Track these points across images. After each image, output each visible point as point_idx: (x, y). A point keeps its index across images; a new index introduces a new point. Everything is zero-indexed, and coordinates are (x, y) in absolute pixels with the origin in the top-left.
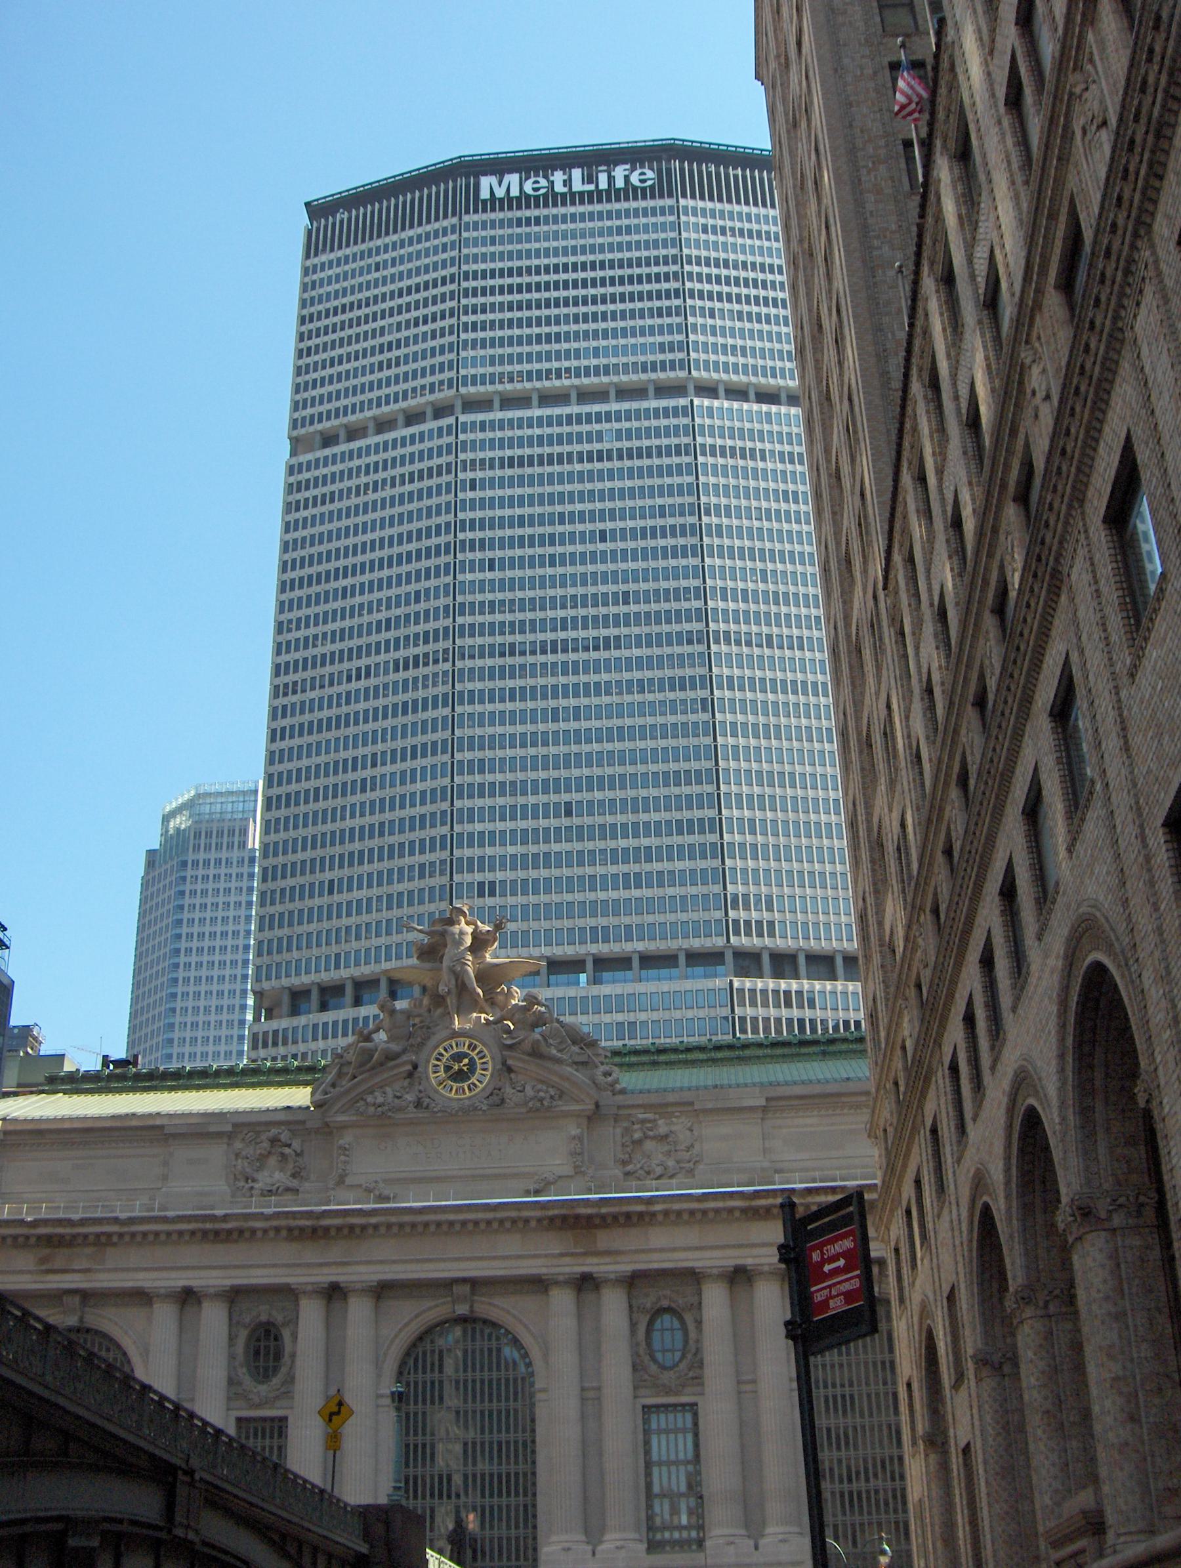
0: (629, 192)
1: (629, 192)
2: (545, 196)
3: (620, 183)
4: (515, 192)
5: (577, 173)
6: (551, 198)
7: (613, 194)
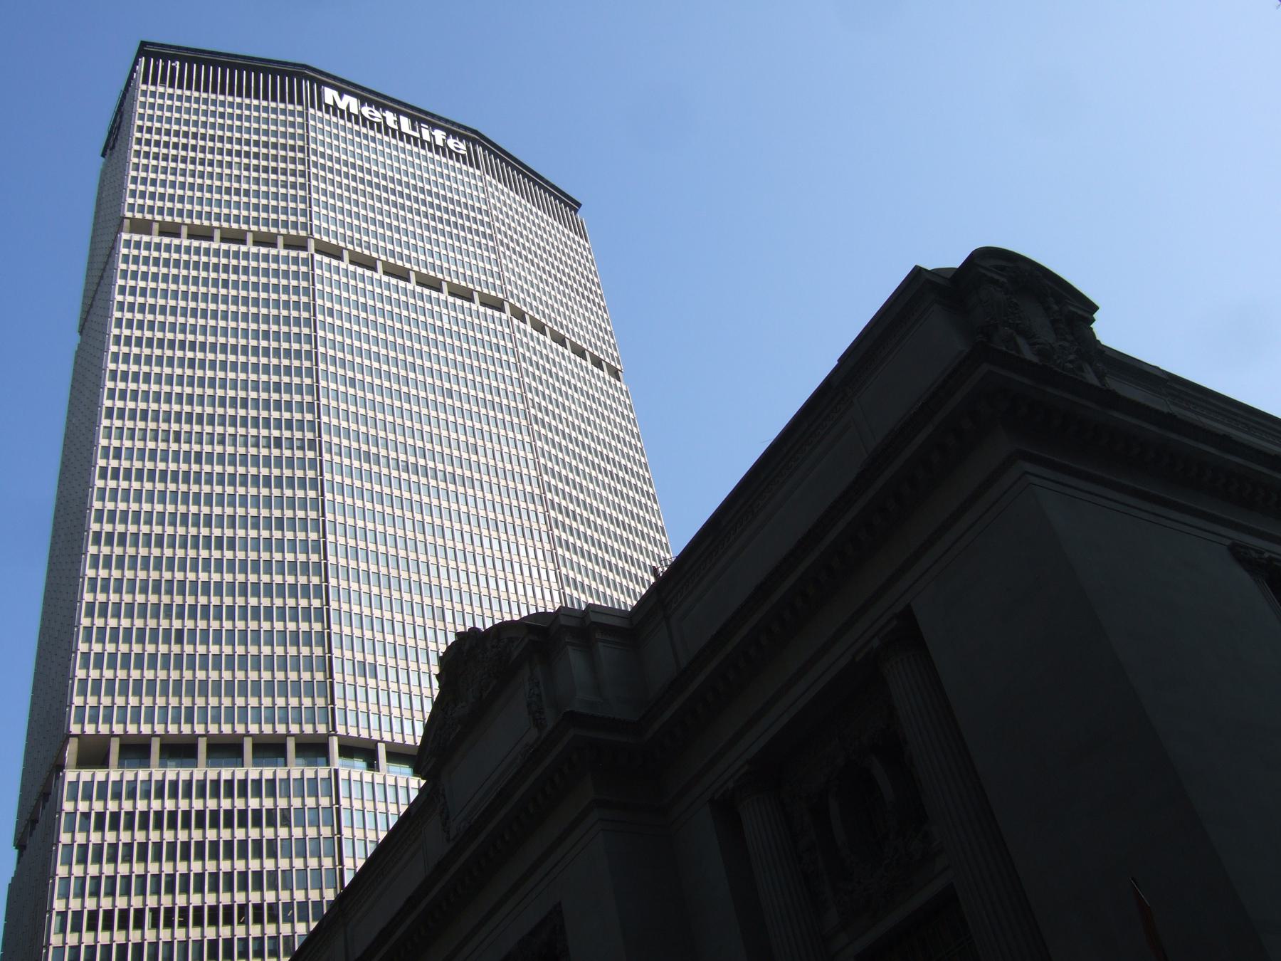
0: (444, 150)
1: (444, 150)
5: (405, 122)
6: (383, 128)
7: (431, 146)
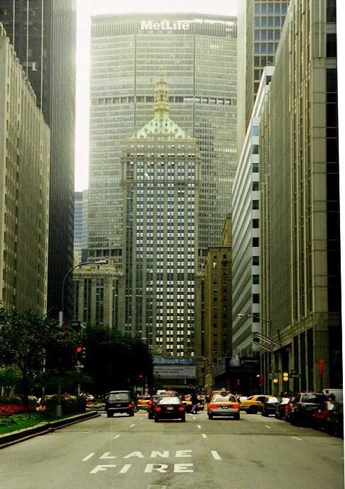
5: (168, 22)
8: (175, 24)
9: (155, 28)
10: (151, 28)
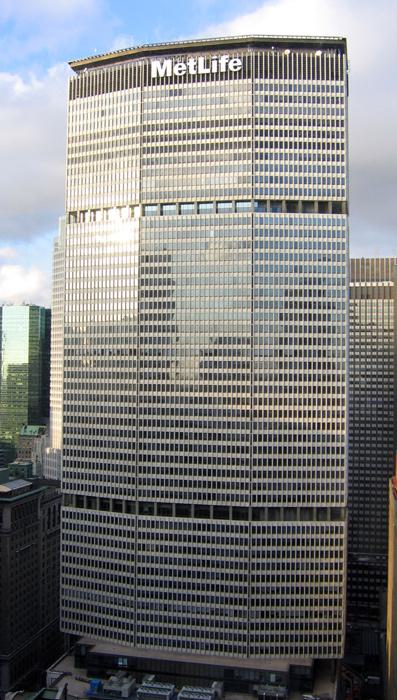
0: (227, 75)
2: (185, 75)
3: (223, 69)
4: (169, 74)
5: (201, 60)
6: (186, 78)
8: (215, 63)
9: (178, 74)
10: (169, 74)
